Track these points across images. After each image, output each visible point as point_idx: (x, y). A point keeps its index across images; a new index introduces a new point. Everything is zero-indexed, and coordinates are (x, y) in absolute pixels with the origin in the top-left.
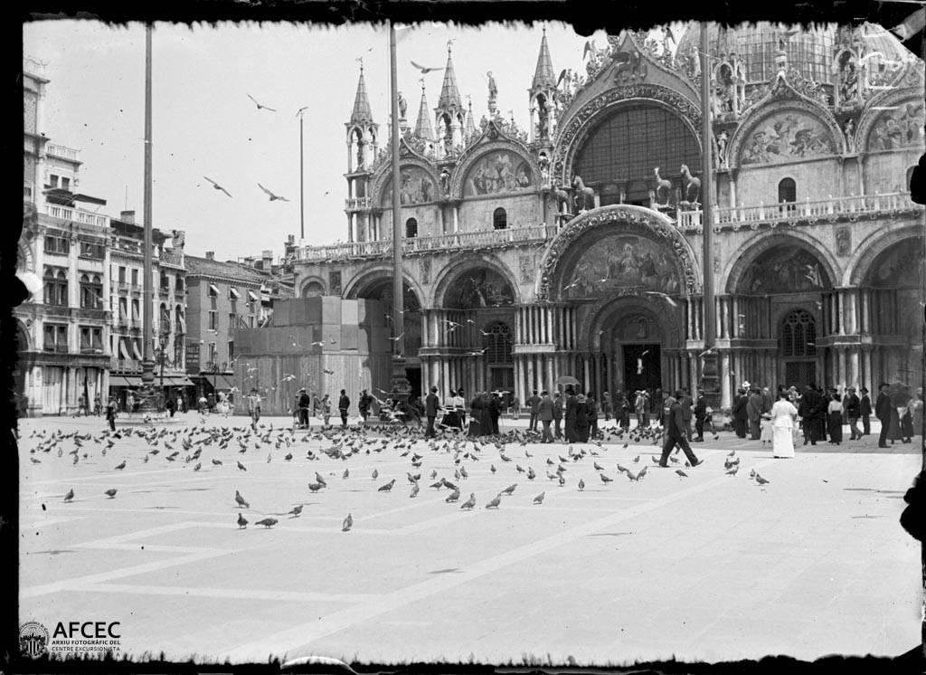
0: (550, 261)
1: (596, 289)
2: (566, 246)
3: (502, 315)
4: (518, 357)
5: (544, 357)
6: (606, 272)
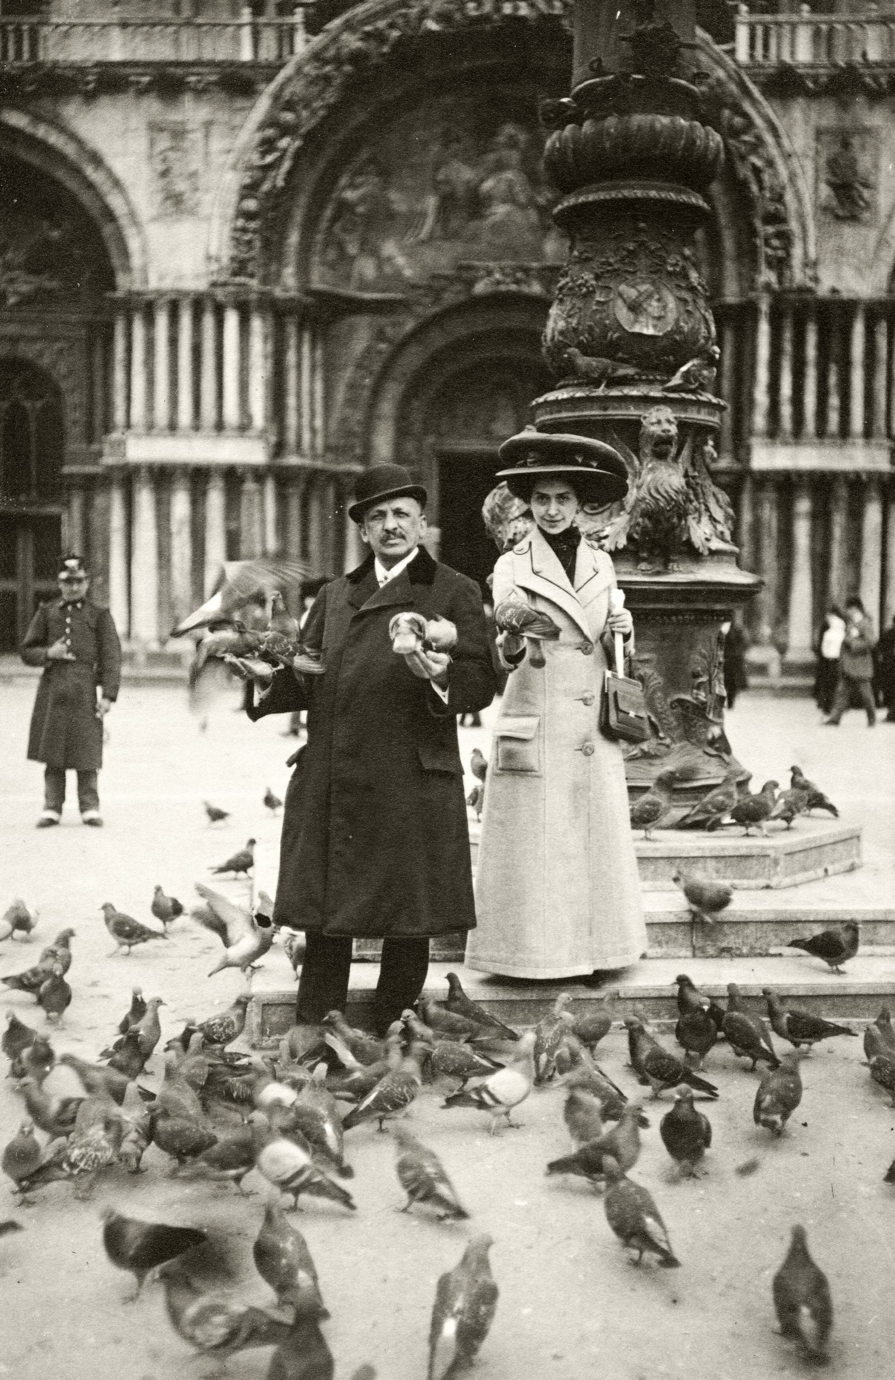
0: (267, 145)
1: (388, 270)
2: (331, 97)
3: (33, 340)
4: (128, 478)
5: (233, 477)
6: (423, 215)
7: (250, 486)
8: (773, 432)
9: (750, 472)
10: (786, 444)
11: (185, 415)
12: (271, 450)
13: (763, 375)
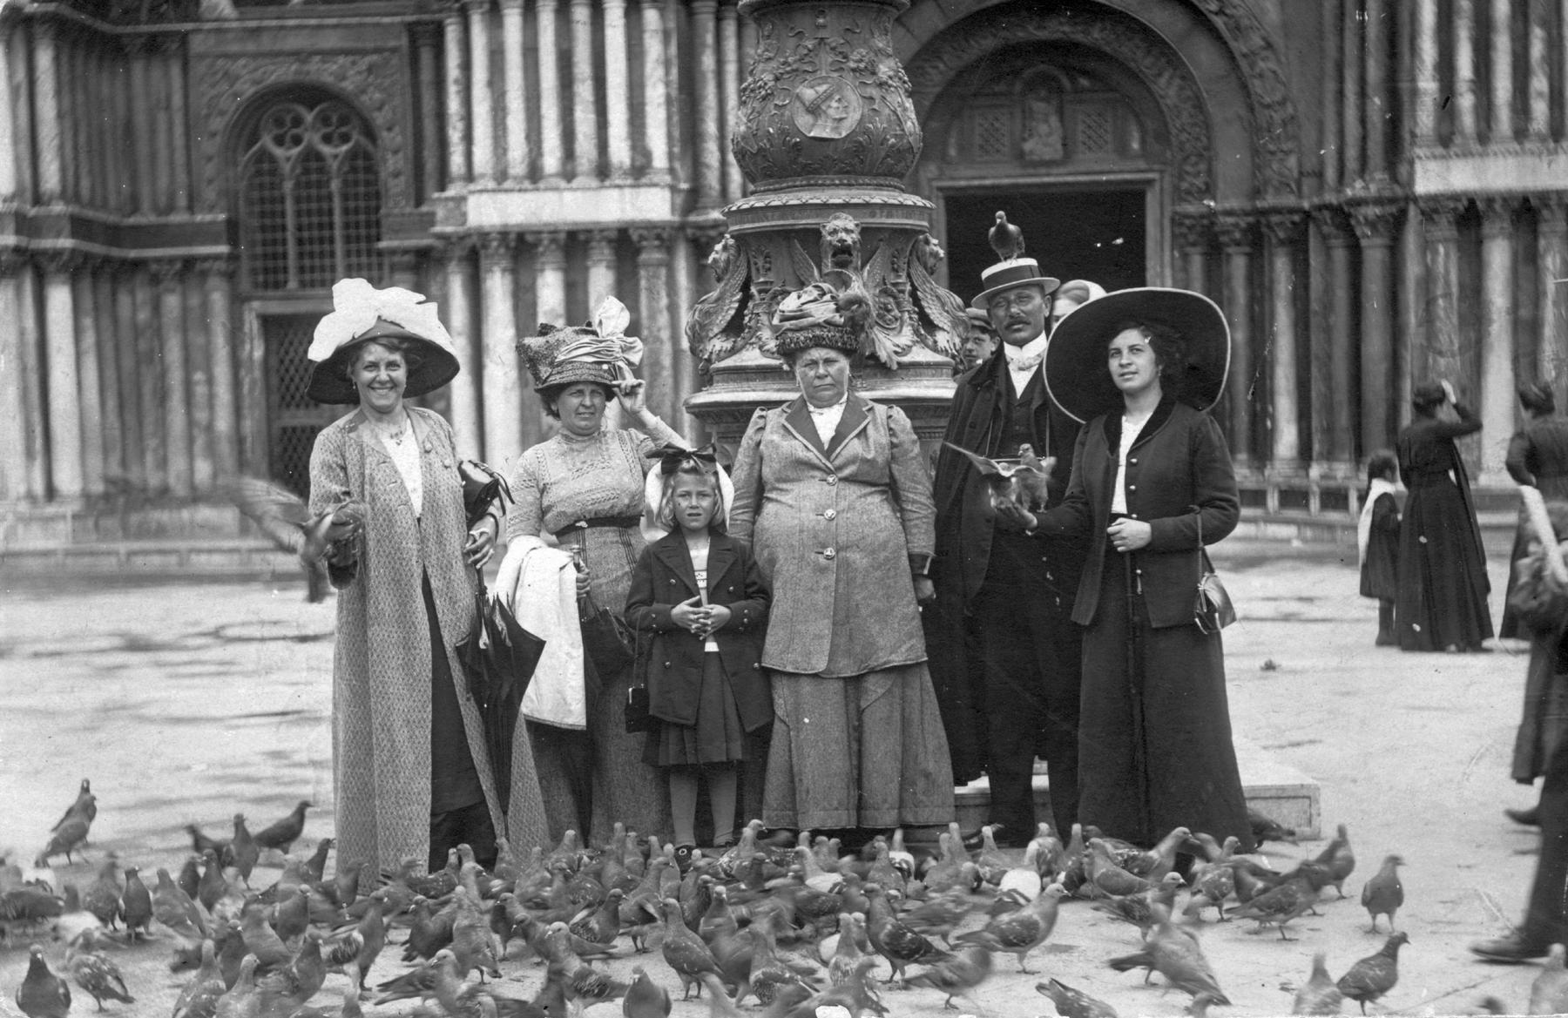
3: (328, 54)
5: (626, 245)
7: (651, 255)
8: (1446, 138)
9: (1415, 199)
10: (1466, 154)
11: (551, 160)
12: (679, 200)
13: (1428, 50)
